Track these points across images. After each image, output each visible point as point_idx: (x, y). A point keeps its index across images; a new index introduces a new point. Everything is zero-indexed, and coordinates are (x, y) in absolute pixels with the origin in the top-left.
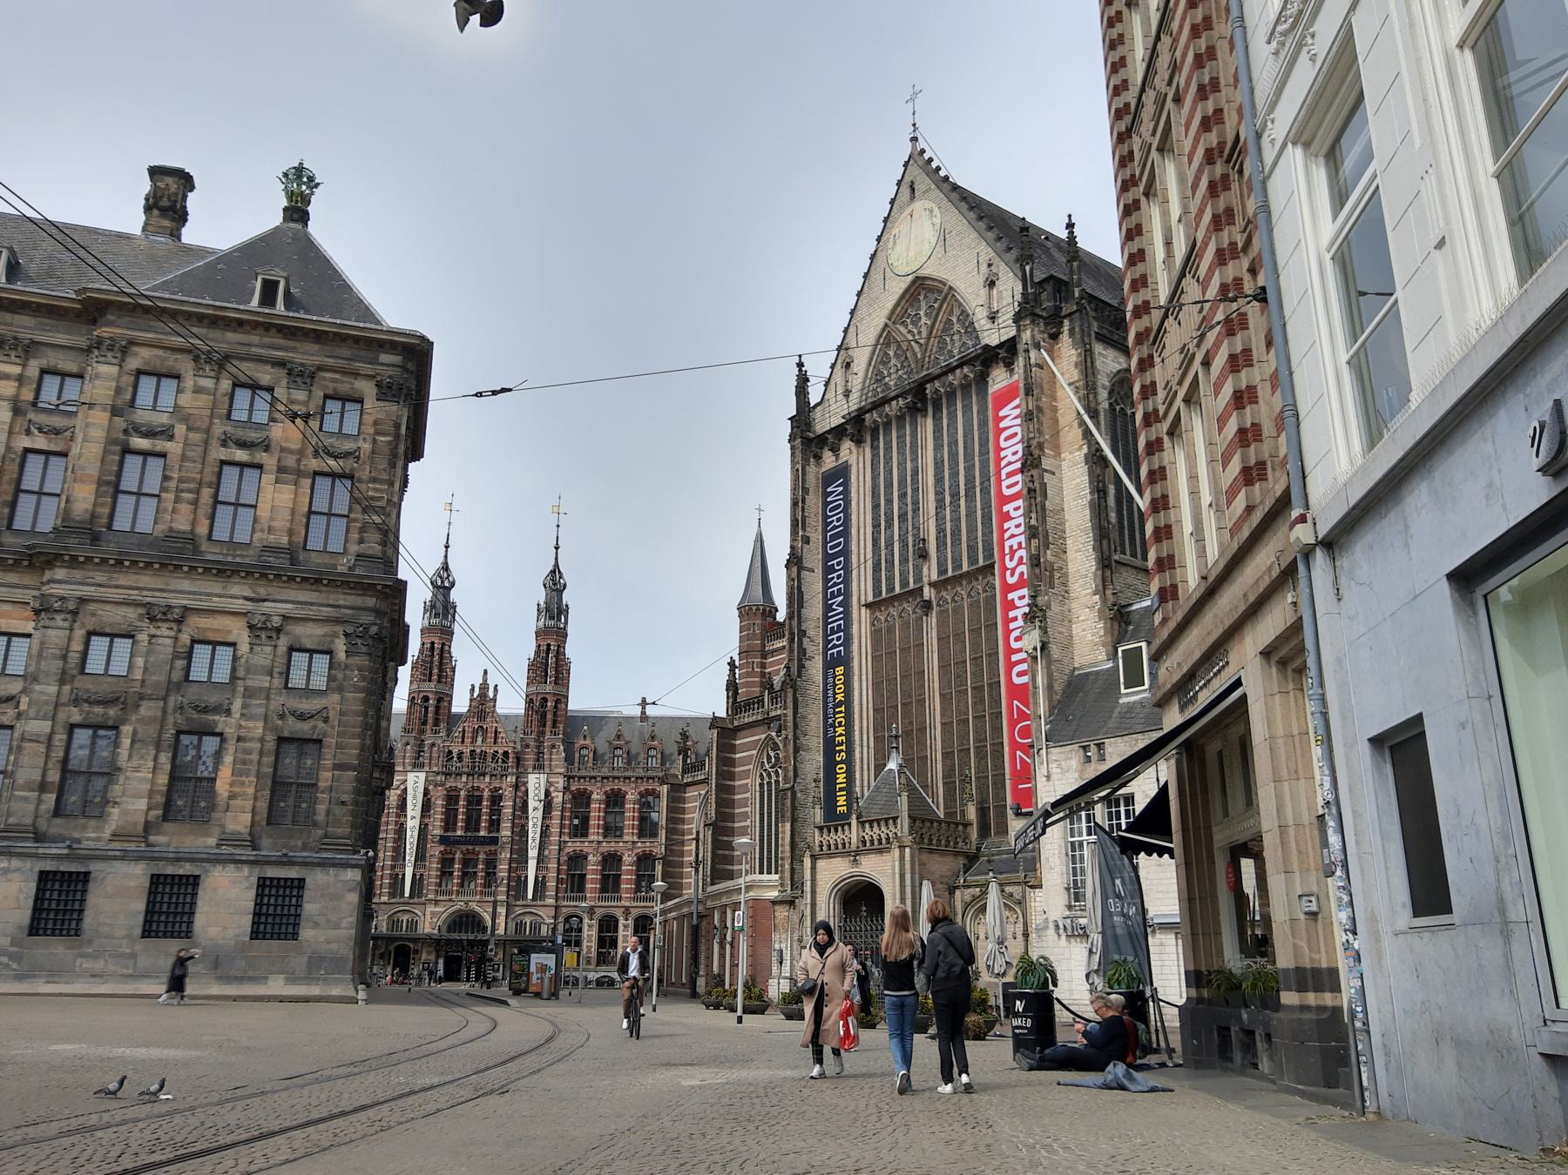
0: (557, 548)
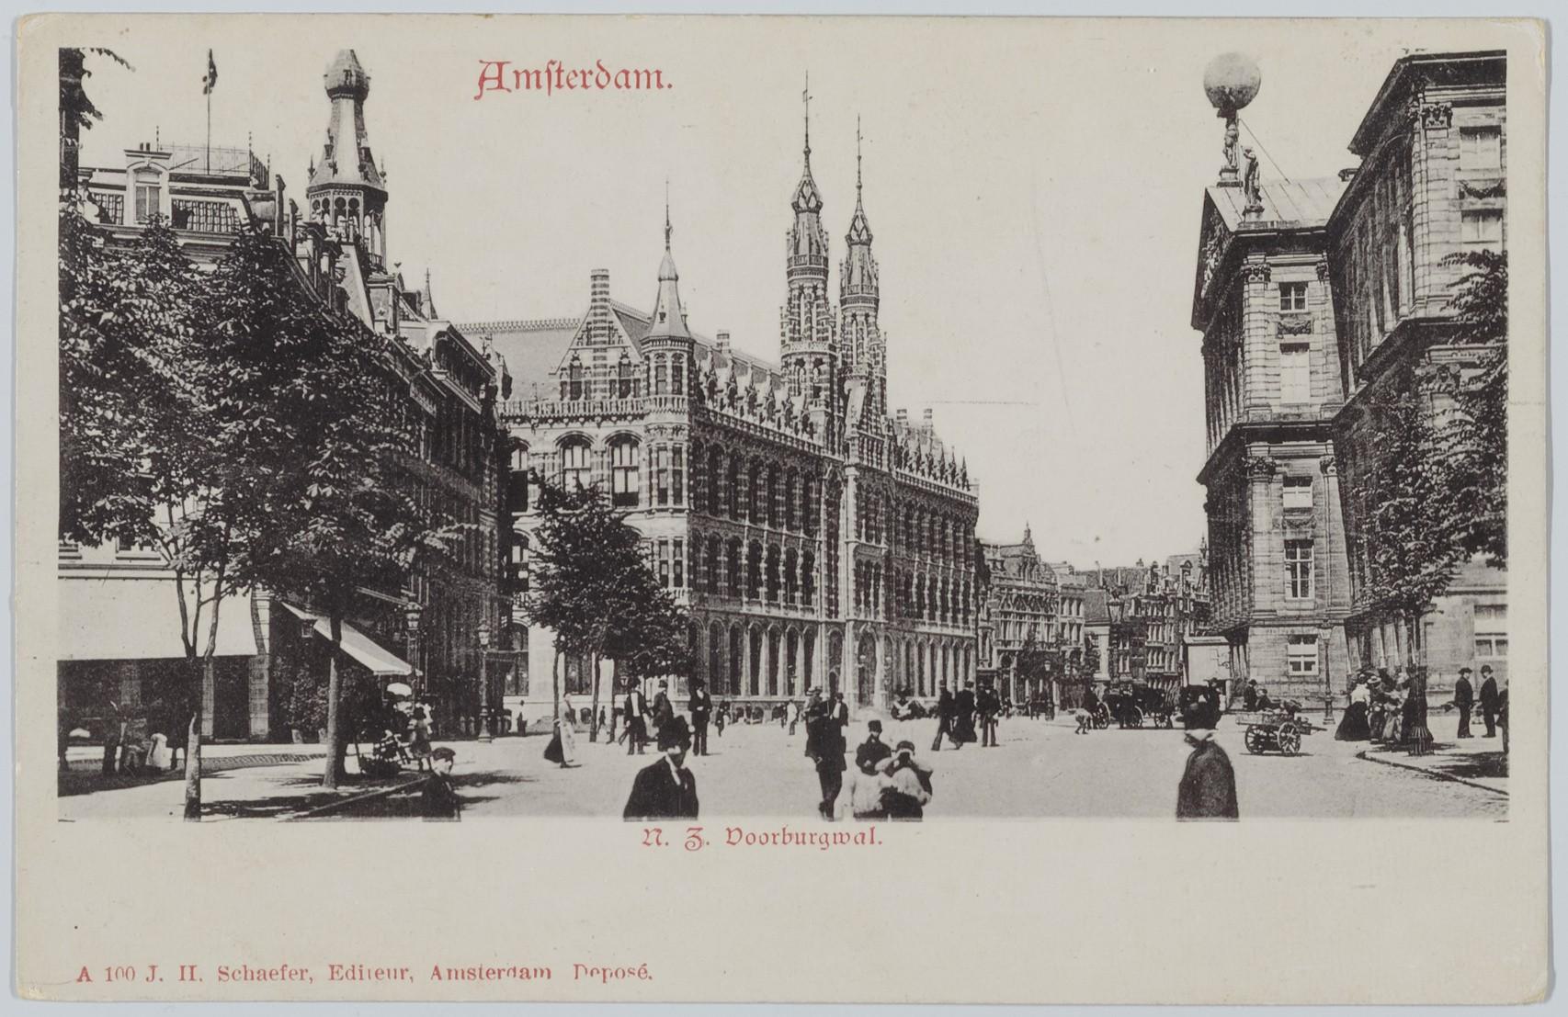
0: (860, 187)
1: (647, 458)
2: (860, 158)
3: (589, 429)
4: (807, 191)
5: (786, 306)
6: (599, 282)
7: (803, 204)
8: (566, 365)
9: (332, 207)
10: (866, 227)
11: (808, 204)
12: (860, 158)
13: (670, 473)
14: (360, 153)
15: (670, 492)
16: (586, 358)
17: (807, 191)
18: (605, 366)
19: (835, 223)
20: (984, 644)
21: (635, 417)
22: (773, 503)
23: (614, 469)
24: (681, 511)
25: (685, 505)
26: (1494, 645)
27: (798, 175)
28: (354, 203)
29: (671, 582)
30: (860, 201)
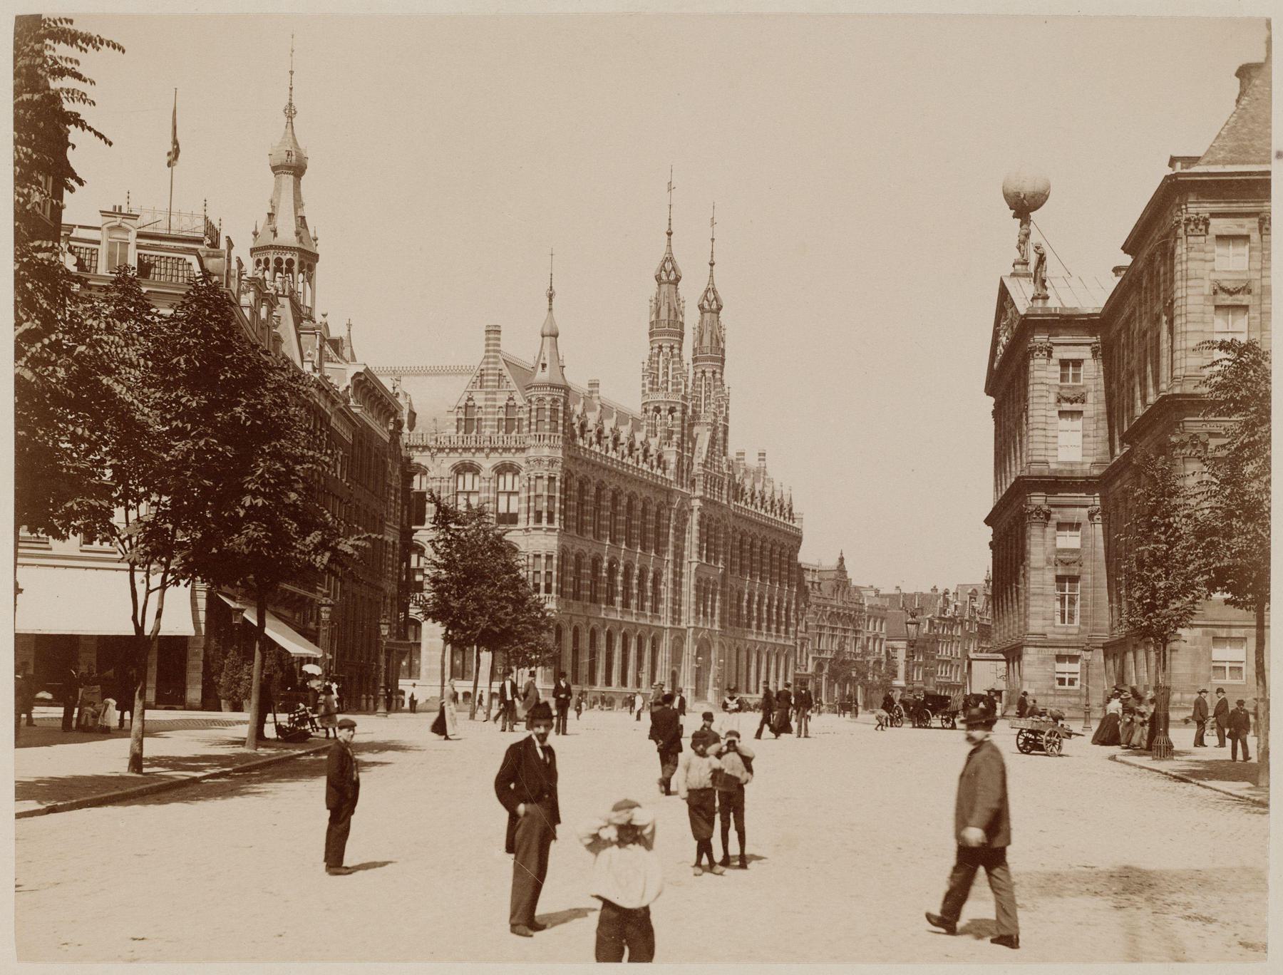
1: (527, 484)
2: (713, 240)
3: (479, 459)
4: (669, 266)
5: (647, 361)
6: (492, 336)
7: (664, 277)
8: (462, 404)
9: (272, 265)
10: (716, 299)
11: (669, 277)
12: (713, 240)
13: (545, 498)
14: (297, 221)
15: (545, 514)
16: (479, 399)
17: (669, 266)
18: (494, 406)
19: (690, 292)
20: (802, 651)
21: (517, 450)
22: (629, 526)
23: (498, 493)
24: (554, 530)
25: (556, 525)
26: (1227, 669)
27: (662, 254)
28: (290, 262)
29: (542, 589)
30: (711, 276)
